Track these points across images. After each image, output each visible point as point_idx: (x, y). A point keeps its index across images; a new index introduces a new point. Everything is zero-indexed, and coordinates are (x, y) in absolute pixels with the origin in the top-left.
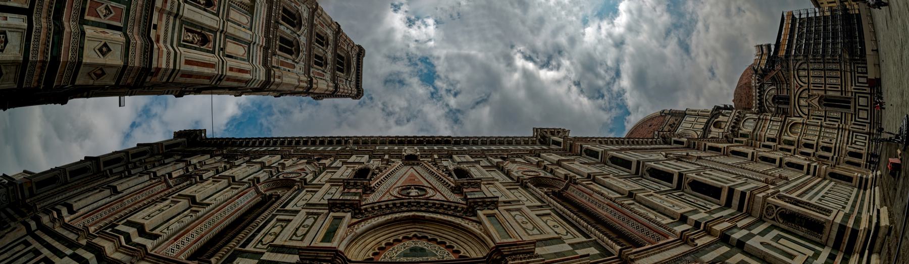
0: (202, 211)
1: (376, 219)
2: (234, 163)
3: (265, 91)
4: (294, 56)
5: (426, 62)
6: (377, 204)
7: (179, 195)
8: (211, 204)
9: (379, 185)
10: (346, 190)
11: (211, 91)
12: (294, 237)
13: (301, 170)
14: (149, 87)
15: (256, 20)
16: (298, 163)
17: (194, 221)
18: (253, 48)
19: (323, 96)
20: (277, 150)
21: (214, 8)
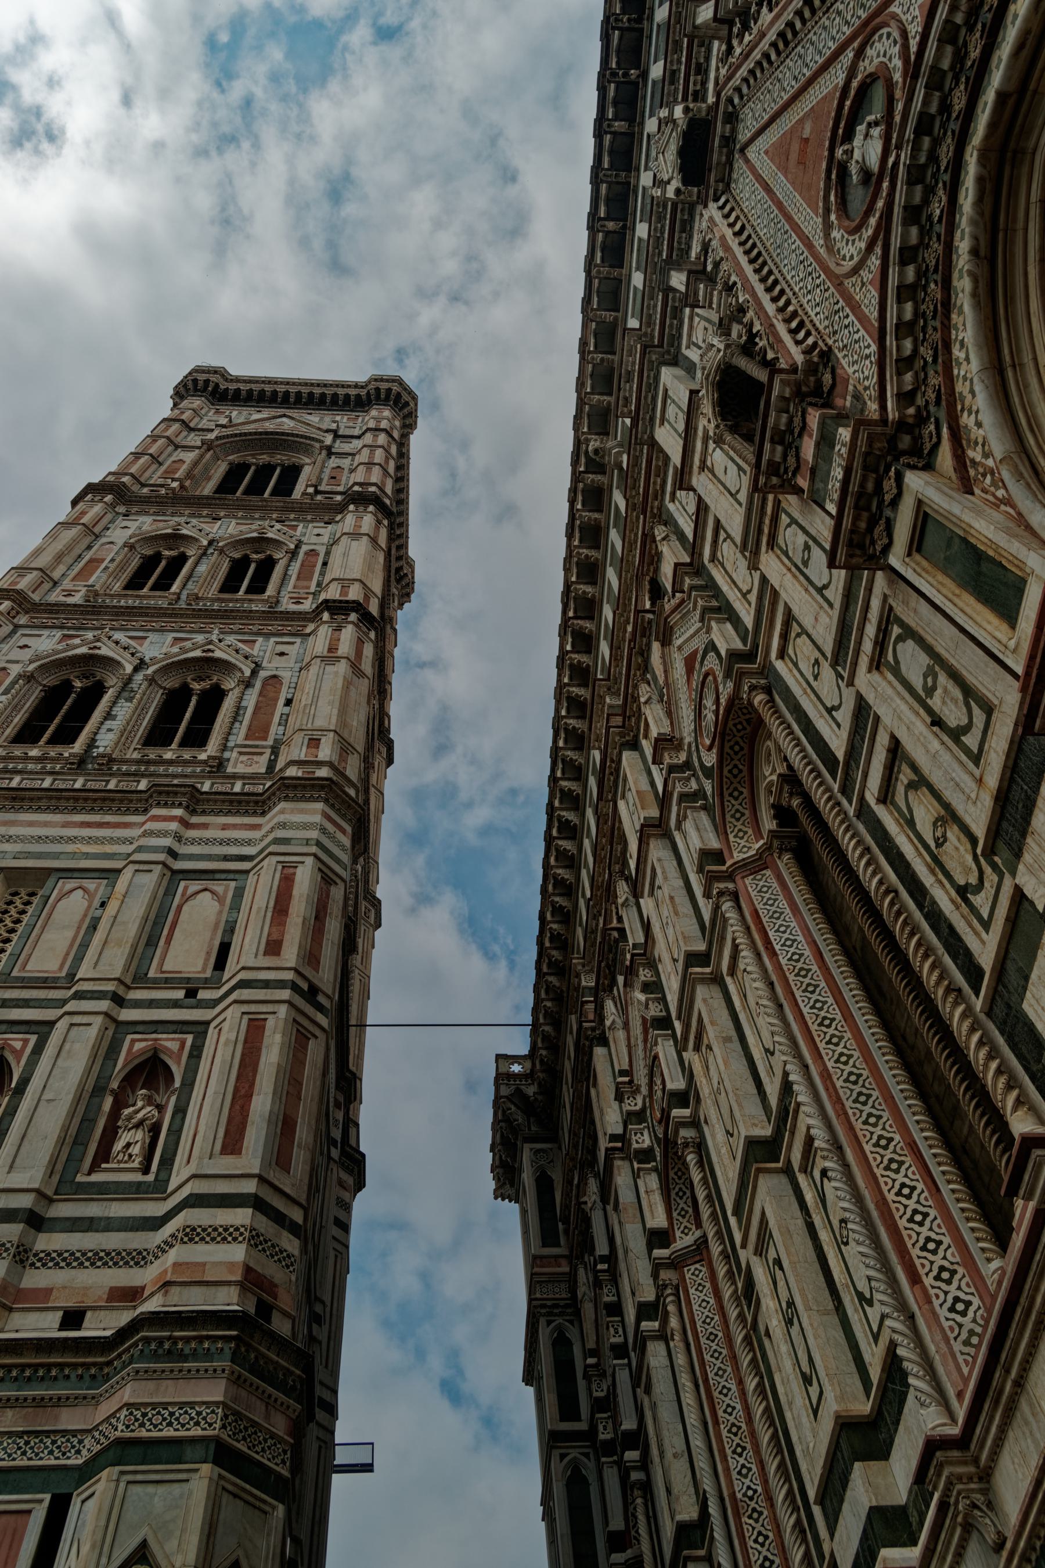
0: (808, 1120)
1: (957, 353)
2: (635, 946)
3: (367, 801)
4: (229, 683)
5: (233, 48)
6: (890, 341)
7: (737, 1211)
8: (786, 1074)
9: (801, 325)
10: (803, 483)
11: (352, 1030)
12: (971, 740)
13: (690, 670)
14: (316, 1319)
15: (73, 855)
16: (661, 680)
17: (846, 1165)
18: (191, 857)
19: (399, 558)
20: (603, 761)
21: (14, 1051)
